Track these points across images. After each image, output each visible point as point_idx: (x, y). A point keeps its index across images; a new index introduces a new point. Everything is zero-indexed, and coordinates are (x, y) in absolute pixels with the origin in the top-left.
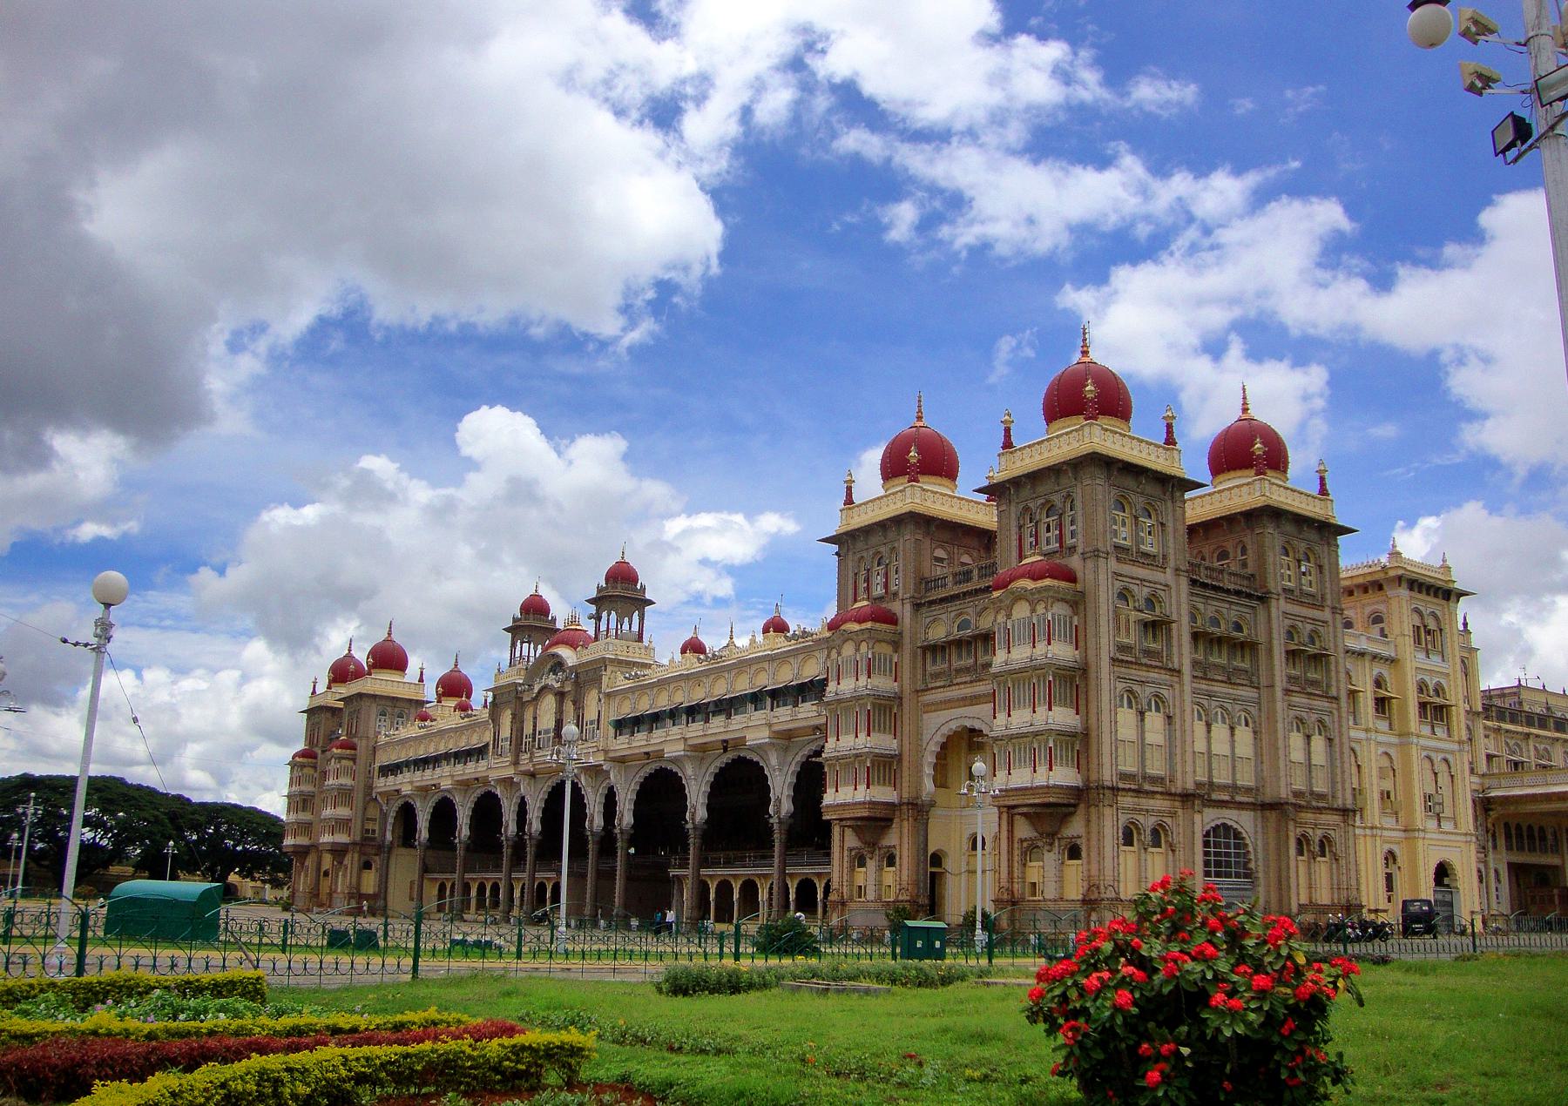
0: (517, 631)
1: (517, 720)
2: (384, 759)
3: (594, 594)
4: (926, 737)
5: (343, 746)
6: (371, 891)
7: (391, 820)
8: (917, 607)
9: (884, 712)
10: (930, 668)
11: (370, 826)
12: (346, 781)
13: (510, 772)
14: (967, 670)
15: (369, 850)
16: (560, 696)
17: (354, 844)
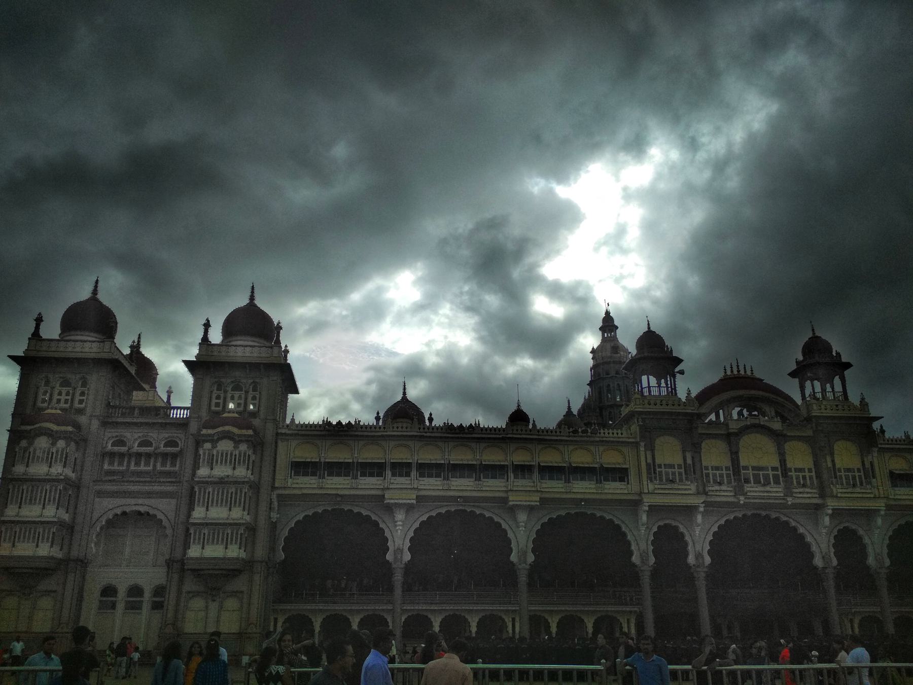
2: (307, 454)
16: (779, 438)
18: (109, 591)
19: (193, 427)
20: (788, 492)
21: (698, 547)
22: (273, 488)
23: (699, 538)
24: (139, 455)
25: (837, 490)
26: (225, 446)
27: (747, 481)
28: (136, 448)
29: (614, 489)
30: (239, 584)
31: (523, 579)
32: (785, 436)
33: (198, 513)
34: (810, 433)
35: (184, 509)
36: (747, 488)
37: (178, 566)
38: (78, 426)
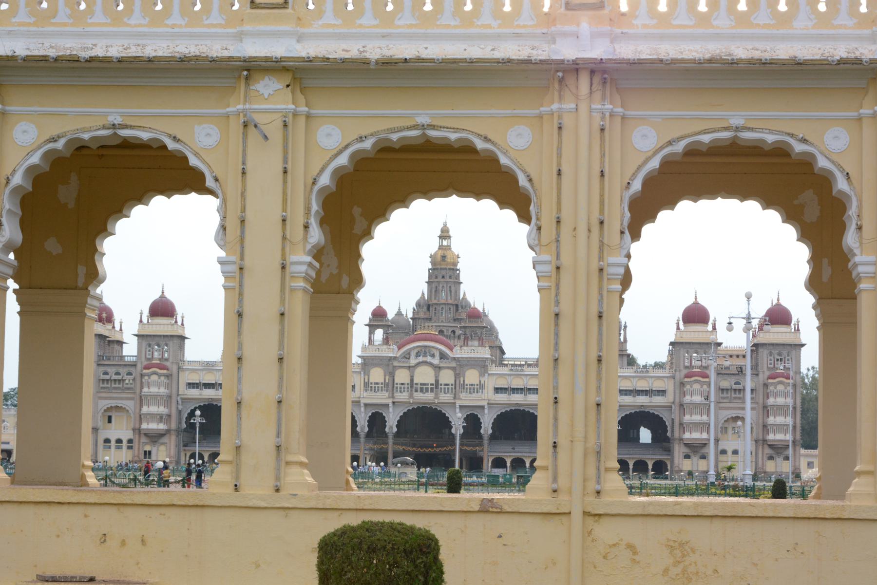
0: (372, 327)
2: (195, 379)
14: (740, 398)
16: (437, 368)
18: (107, 441)
19: (139, 366)
20: (437, 397)
21: (391, 423)
23: (392, 420)
24: (115, 380)
25: (463, 395)
26: (154, 378)
27: (416, 391)
28: (114, 377)
30: (165, 439)
32: (440, 368)
33: (145, 409)
34: (454, 364)
35: (138, 406)
37: (138, 431)
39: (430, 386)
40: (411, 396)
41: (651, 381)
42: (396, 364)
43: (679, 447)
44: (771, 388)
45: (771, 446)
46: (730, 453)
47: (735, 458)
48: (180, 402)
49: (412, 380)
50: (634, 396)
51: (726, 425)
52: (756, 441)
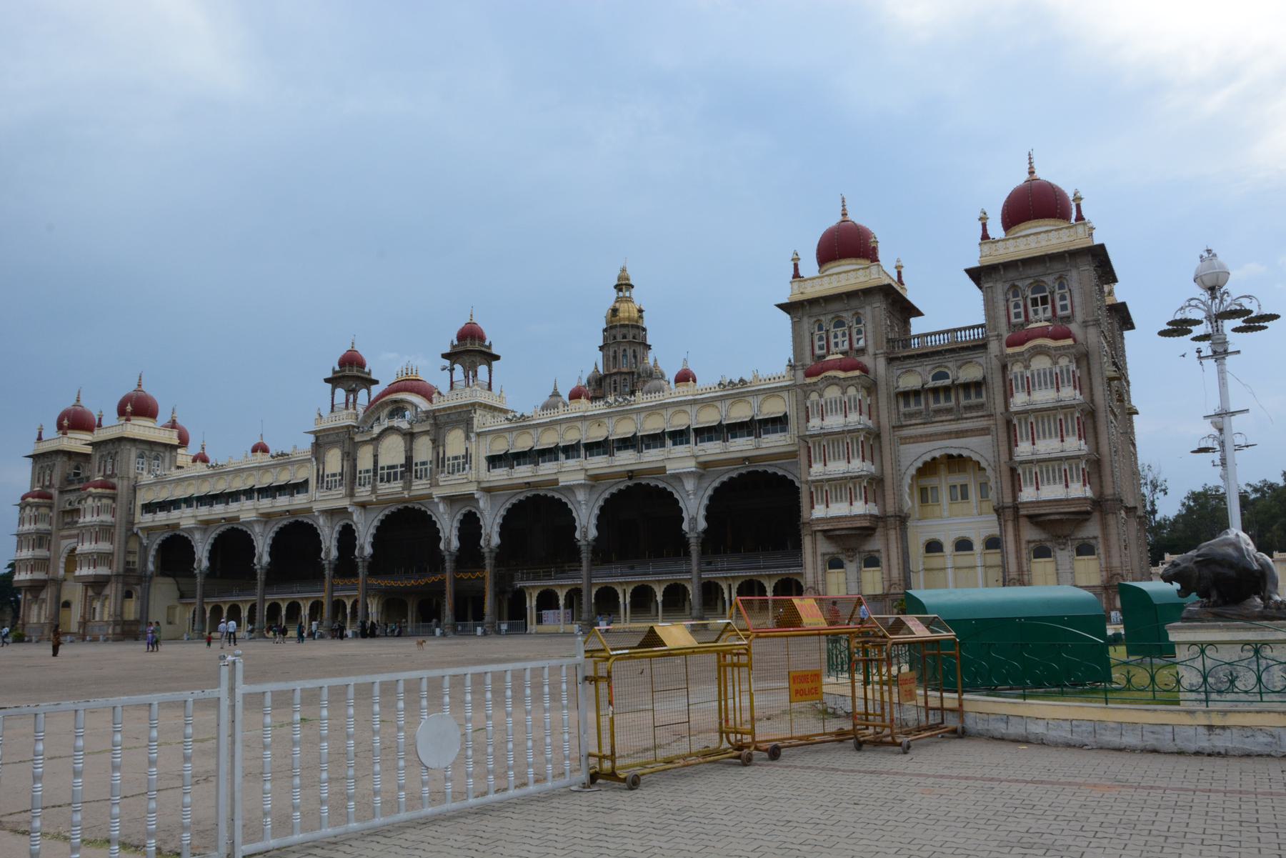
1: (350, 457)
3: (448, 350)
4: (905, 462)
5: (103, 485)
6: (132, 617)
7: (153, 552)
8: (891, 360)
9: (872, 441)
10: (902, 409)
11: (131, 559)
12: (106, 518)
13: (345, 503)
14: (949, 411)
15: (132, 581)
16: (410, 436)
17: (118, 575)
22: (133, 524)
25: (442, 478)
26: (90, 500)
27: (382, 480)
29: (299, 500)
31: (260, 577)
36: (380, 485)
38: (50, 497)
39: (399, 470)
40: (374, 490)
41: (755, 401)
42: (358, 438)
43: (814, 543)
44: (1017, 369)
45: (1035, 520)
46: (948, 548)
47: (964, 559)
48: (140, 533)
49: (376, 463)
50: (725, 440)
51: (929, 482)
52: (999, 511)
